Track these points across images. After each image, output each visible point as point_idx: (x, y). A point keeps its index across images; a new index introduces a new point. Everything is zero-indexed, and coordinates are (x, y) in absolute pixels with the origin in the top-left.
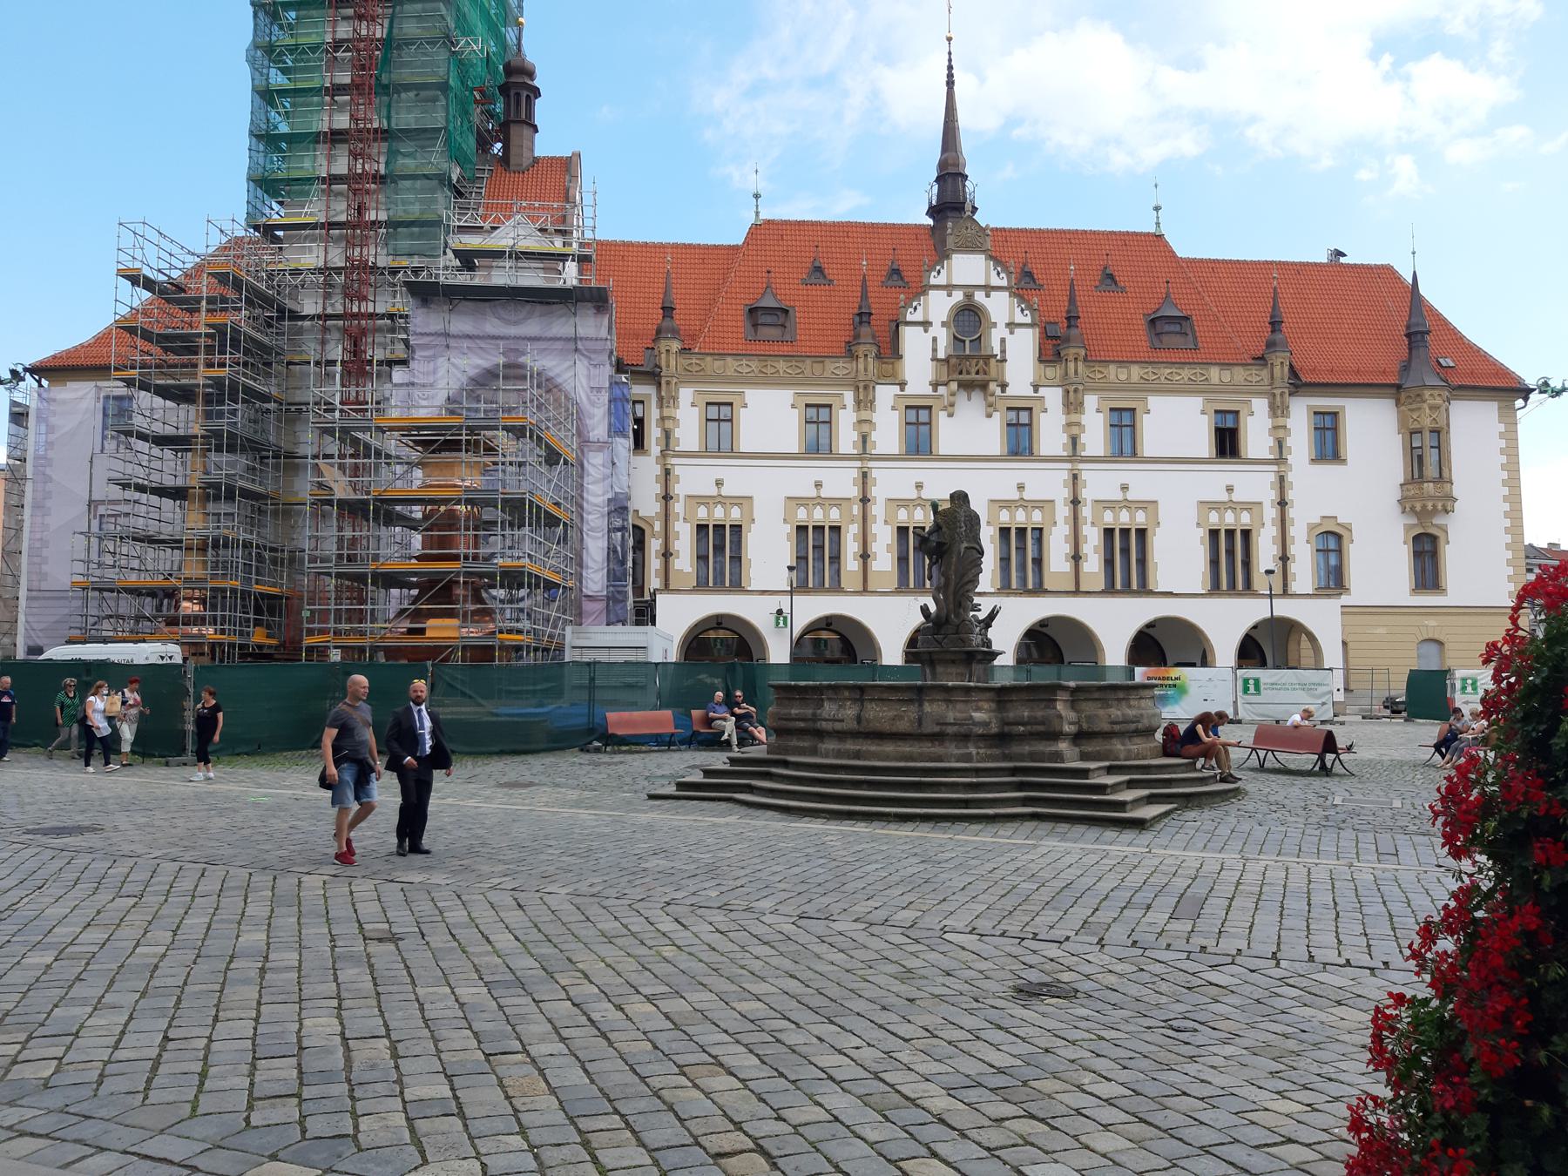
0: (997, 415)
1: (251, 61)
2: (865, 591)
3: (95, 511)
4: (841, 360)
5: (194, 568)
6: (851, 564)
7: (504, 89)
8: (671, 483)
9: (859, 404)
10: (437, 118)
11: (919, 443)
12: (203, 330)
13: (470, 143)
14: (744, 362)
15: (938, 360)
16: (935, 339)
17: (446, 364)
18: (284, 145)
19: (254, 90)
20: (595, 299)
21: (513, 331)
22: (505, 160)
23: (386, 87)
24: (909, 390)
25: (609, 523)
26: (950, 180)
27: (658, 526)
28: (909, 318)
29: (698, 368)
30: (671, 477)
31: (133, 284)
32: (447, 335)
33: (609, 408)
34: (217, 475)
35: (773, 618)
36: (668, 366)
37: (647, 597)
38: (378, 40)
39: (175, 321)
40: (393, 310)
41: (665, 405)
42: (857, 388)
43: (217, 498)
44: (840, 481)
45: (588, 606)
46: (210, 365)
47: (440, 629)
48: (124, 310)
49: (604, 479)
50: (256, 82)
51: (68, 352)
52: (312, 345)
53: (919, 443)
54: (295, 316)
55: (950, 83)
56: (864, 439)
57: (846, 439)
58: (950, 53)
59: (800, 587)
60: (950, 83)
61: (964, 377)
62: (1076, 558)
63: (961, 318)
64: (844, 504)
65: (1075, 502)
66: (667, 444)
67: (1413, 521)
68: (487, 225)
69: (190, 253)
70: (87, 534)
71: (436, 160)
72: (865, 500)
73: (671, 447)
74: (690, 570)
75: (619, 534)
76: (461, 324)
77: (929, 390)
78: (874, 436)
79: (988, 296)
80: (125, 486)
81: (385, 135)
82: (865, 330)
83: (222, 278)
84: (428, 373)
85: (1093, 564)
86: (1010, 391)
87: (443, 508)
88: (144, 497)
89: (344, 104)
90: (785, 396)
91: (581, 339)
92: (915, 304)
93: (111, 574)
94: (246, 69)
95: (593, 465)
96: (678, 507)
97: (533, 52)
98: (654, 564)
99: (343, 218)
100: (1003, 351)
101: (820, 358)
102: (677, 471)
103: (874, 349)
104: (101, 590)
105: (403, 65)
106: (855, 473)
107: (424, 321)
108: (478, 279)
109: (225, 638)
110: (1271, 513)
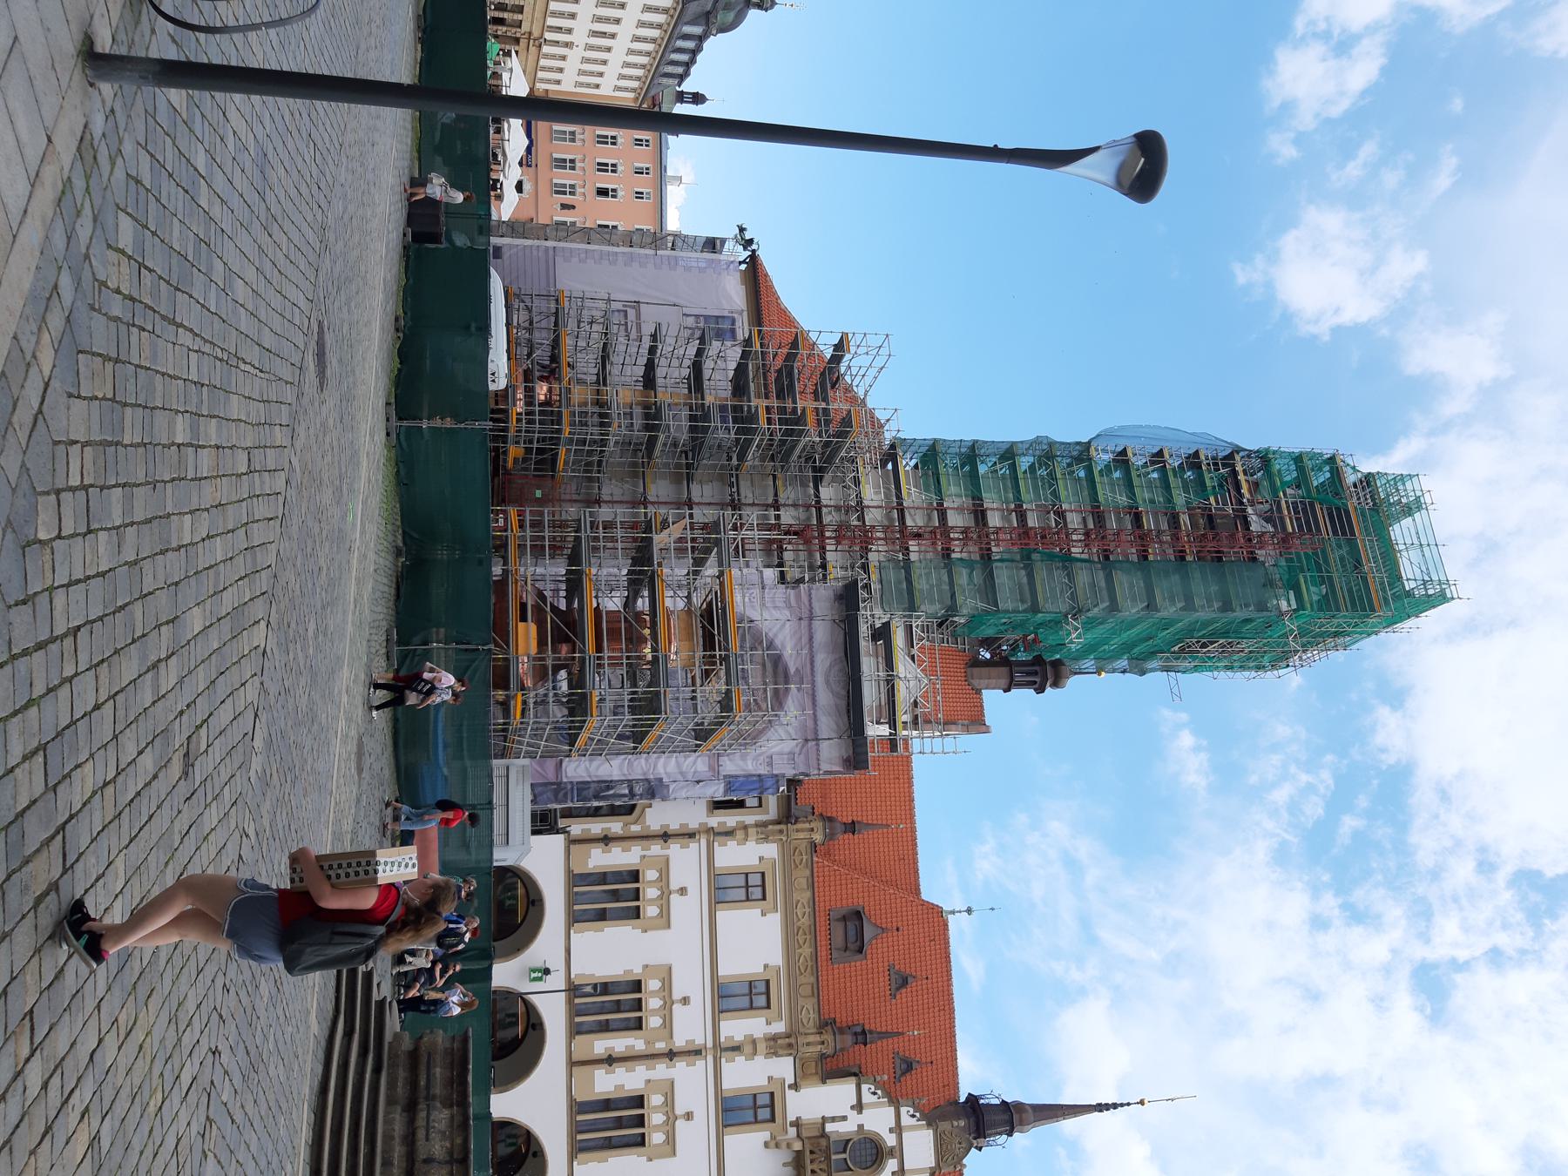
1: (1037, 441)
2: (572, 1064)
3: (630, 306)
4: (817, 1016)
5: (579, 394)
6: (601, 1045)
7: (1038, 660)
8: (681, 840)
9: (773, 1038)
10: (1007, 601)
12: (799, 406)
13: (989, 632)
14: (807, 910)
15: (823, 1125)
16: (844, 1118)
17: (785, 618)
18: (967, 468)
19: (1013, 444)
20: (856, 758)
21: (820, 679)
22: (976, 663)
23: (1029, 558)
24: (790, 1094)
25: (637, 781)
26: (1006, 1117)
27: (635, 828)
28: (865, 1087)
29: (797, 862)
30: (686, 840)
31: (835, 345)
32: (811, 618)
33: (754, 775)
34: (667, 414)
35: (540, 964)
36: (797, 831)
37: (562, 823)
38: (1069, 550)
39: (805, 382)
40: (830, 567)
41: (759, 830)
42: (789, 1036)
43: (647, 416)
44: (690, 1026)
45: (550, 764)
46: (768, 410)
47: (526, 636)
48: (813, 336)
49: (681, 773)
50: (1020, 445)
51: (772, 287)
52: (792, 496)
54: (817, 482)
55: (1101, 1108)
56: (737, 1049)
57: (736, 1028)
58: (1128, 1104)
59: (573, 990)
60: (1101, 1108)
61: (808, 1157)
63: (868, 1145)
64: (666, 1032)
66: (720, 834)
68: (915, 651)
69: (866, 392)
70: (609, 300)
71: (969, 604)
72: (671, 1055)
73: (718, 838)
75: (627, 791)
76: (823, 631)
77: (791, 1117)
78: (740, 1059)
80: (654, 337)
81: (986, 557)
82: (849, 1039)
83: (847, 421)
84: (774, 602)
87: (647, 632)
88: (644, 351)
89: (1010, 521)
90: (776, 958)
91: (818, 745)
92: (879, 1092)
93: (572, 324)
94: (1029, 436)
95: (695, 763)
96: (656, 849)
97: (1073, 682)
98: (596, 827)
99: (909, 522)
101: (817, 992)
102: (694, 846)
103: (830, 1051)
104: (556, 313)
105: (1050, 572)
106: (699, 1041)
107: (822, 597)
108: (865, 645)
109: (513, 423)
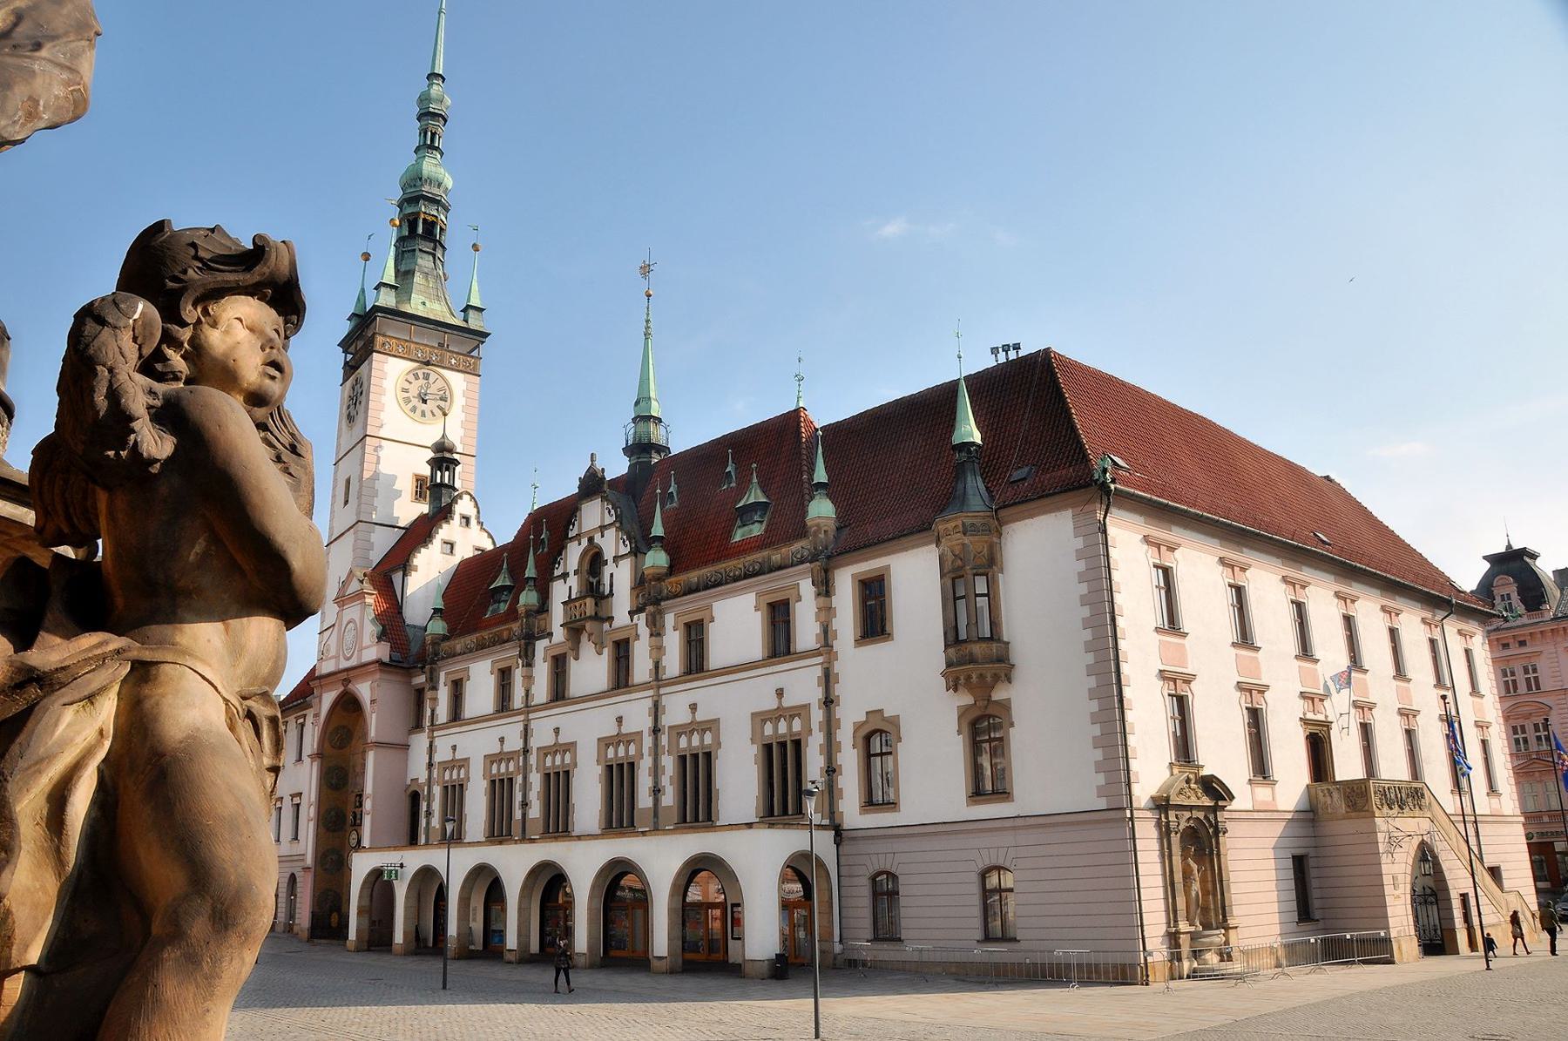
0: (606, 651)
6: (518, 814)
11: (559, 693)
16: (570, 587)
53: (559, 693)
62: (657, 791)
65: (656, 731)
67: (966, 699)
72: (526, 751)
74: (437, 827)
79: (603, 536)
85: (669, 798)
86: (616, 624)
100: (611, 590)
110: (817, 715)
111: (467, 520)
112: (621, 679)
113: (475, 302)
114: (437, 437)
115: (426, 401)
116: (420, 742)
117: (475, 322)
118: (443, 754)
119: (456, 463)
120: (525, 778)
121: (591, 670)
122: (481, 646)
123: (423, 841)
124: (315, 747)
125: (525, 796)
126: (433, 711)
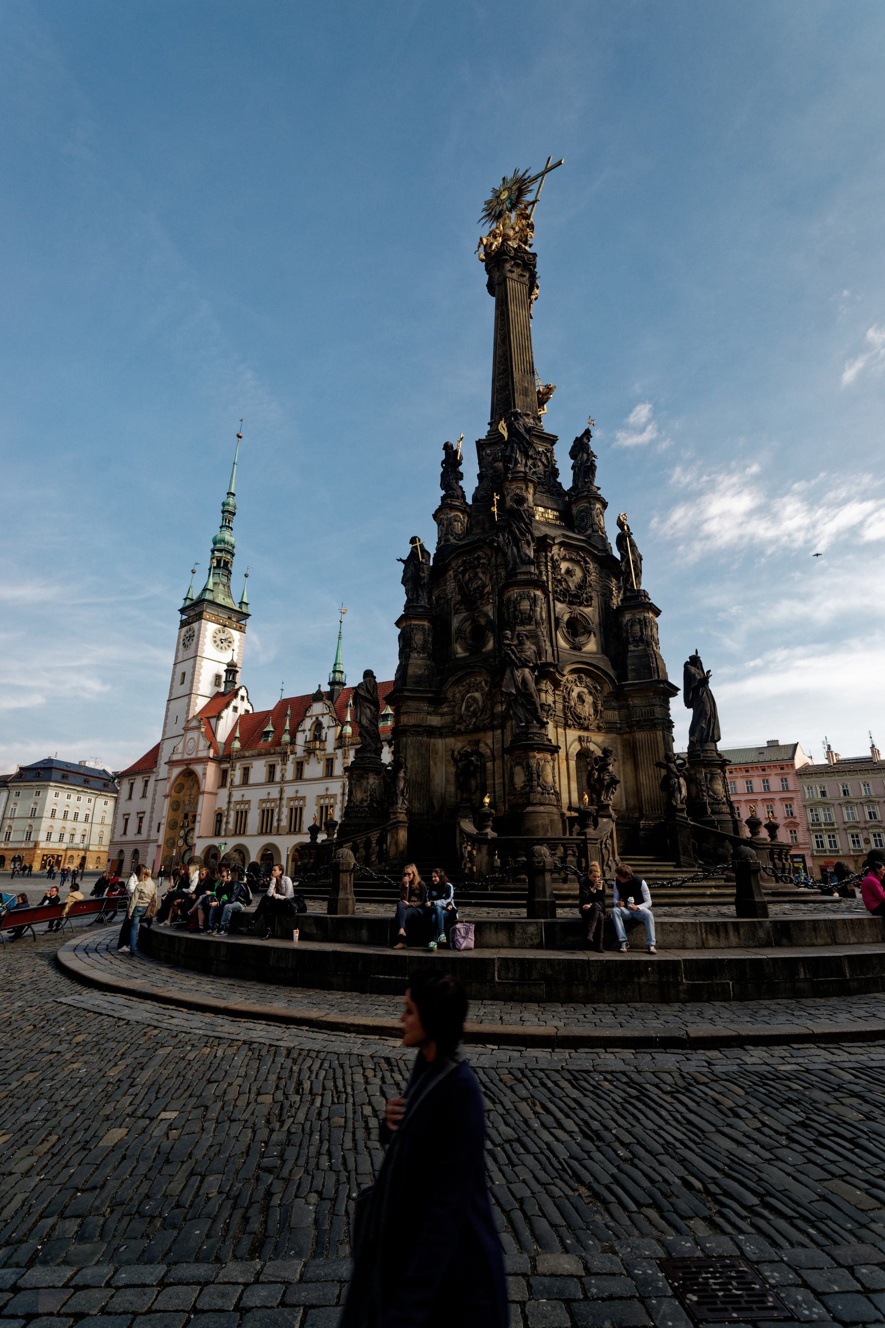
0: (322, 762)
6: (275, 824)
11: (299, 775)
24: (298, 755)
44: (275, 793)
53: (299, 775)
55: (340, 638)
56: (283, 775)
60: (340, 638)
72: (281, 799)
96: (232, 806)
102: (233, 793)
106: (279, 789)
111: (242, 698)
112: (329, 773)
113: (245, 600)
114: (228, 660)
115: (224, 643)
116: (224, 792)
117: (244, 610)
118: (237, 796)
119: (237, 672)
120: (280, 810)
121: (315, 768)
122: (260, 755)
123: (223, 833)
124: (167, 791)
125: (279, 816)
126: (232, 780)
